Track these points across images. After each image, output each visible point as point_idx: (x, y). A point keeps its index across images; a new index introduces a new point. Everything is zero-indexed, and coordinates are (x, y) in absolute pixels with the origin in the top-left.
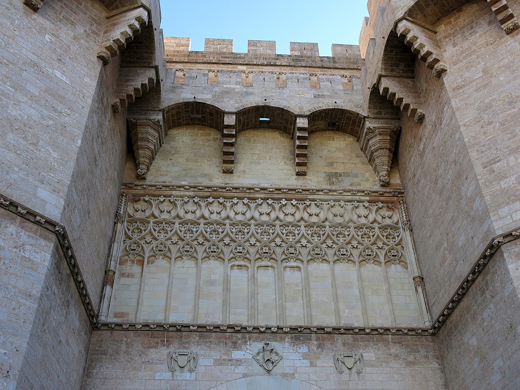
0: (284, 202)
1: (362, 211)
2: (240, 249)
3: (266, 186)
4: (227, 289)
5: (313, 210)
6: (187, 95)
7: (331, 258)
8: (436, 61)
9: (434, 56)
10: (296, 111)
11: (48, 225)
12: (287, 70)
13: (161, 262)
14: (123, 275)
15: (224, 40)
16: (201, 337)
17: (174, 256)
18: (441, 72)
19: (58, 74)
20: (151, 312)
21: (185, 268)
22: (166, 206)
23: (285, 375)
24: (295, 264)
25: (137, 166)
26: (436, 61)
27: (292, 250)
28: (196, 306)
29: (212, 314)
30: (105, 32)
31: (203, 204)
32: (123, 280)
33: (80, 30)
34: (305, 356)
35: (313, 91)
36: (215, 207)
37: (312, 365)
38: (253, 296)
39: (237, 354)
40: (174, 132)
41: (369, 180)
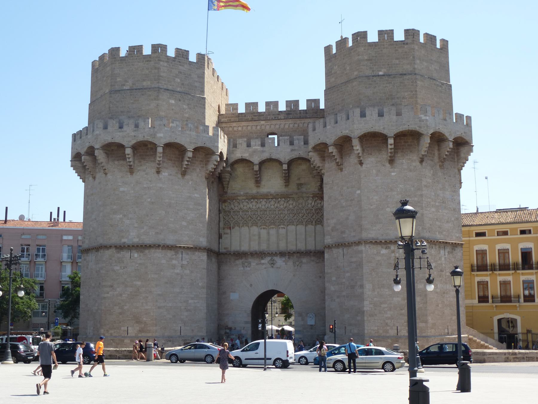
0: (279, 199)
1: (310, 202)
2: (263, 222)
3: (272, 191)
4: (259, 238)
5: (291, 202)
6: (238, 154)
7: (295, 223)
8: (321, 170)
9: (320, 168)
10: (282, 160)
11: (205, 249)
12: (283, 122)
13: (237, 228)
14: (225, 234)
15: (254, 103)
16: (252, 256)
17: (241, 225)
18: (324, 174)
19: (196, 195)
20: (235, 247)
21: (245, 230)
22: (236, 204)
23: (277, 268)
24: (283, 226)
25: (223, 188)
26: (321, 170)
27: (282, 221)
28: (250, 245)
29: (255, 247)
30: (206, 164)
31: (249, 202)
32: (225, 236)
33: (198, 170)
34: (284, 261)
35: (291, 147)
36: (254, 203)
37: (286, 264)
38: (268, 240)
39: (263, 261)
40: (236, 166)
41: (313, 187)
